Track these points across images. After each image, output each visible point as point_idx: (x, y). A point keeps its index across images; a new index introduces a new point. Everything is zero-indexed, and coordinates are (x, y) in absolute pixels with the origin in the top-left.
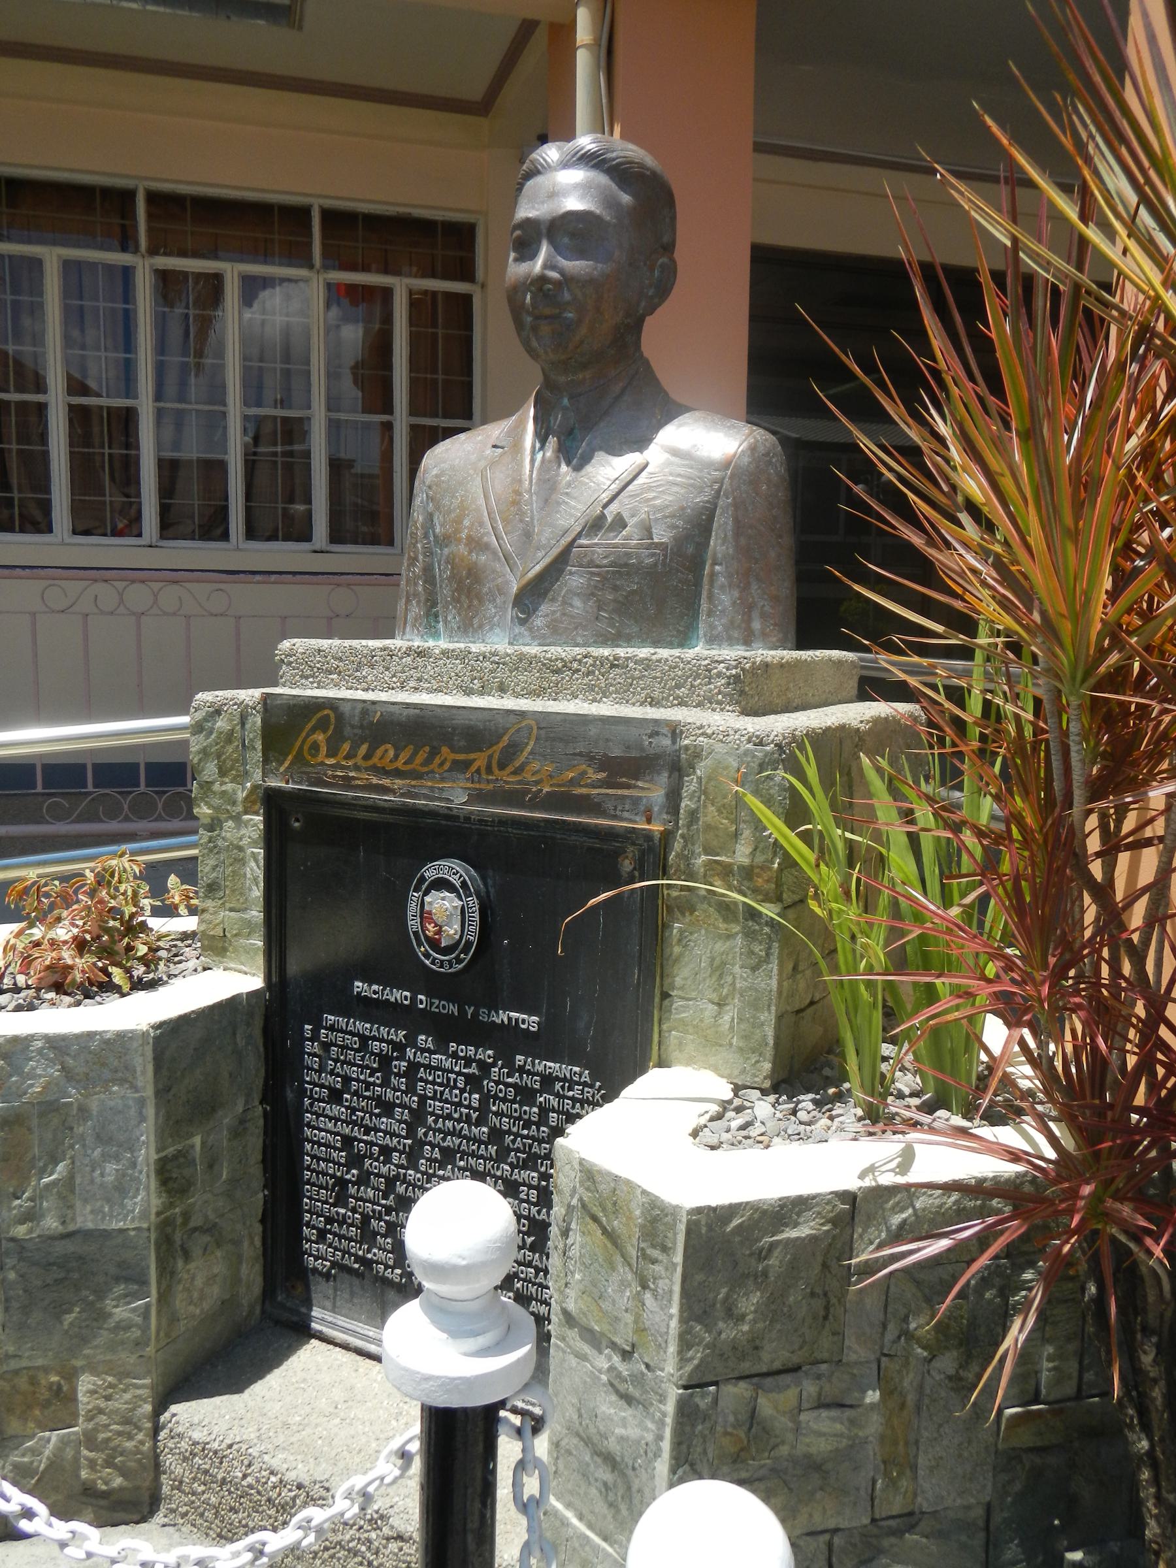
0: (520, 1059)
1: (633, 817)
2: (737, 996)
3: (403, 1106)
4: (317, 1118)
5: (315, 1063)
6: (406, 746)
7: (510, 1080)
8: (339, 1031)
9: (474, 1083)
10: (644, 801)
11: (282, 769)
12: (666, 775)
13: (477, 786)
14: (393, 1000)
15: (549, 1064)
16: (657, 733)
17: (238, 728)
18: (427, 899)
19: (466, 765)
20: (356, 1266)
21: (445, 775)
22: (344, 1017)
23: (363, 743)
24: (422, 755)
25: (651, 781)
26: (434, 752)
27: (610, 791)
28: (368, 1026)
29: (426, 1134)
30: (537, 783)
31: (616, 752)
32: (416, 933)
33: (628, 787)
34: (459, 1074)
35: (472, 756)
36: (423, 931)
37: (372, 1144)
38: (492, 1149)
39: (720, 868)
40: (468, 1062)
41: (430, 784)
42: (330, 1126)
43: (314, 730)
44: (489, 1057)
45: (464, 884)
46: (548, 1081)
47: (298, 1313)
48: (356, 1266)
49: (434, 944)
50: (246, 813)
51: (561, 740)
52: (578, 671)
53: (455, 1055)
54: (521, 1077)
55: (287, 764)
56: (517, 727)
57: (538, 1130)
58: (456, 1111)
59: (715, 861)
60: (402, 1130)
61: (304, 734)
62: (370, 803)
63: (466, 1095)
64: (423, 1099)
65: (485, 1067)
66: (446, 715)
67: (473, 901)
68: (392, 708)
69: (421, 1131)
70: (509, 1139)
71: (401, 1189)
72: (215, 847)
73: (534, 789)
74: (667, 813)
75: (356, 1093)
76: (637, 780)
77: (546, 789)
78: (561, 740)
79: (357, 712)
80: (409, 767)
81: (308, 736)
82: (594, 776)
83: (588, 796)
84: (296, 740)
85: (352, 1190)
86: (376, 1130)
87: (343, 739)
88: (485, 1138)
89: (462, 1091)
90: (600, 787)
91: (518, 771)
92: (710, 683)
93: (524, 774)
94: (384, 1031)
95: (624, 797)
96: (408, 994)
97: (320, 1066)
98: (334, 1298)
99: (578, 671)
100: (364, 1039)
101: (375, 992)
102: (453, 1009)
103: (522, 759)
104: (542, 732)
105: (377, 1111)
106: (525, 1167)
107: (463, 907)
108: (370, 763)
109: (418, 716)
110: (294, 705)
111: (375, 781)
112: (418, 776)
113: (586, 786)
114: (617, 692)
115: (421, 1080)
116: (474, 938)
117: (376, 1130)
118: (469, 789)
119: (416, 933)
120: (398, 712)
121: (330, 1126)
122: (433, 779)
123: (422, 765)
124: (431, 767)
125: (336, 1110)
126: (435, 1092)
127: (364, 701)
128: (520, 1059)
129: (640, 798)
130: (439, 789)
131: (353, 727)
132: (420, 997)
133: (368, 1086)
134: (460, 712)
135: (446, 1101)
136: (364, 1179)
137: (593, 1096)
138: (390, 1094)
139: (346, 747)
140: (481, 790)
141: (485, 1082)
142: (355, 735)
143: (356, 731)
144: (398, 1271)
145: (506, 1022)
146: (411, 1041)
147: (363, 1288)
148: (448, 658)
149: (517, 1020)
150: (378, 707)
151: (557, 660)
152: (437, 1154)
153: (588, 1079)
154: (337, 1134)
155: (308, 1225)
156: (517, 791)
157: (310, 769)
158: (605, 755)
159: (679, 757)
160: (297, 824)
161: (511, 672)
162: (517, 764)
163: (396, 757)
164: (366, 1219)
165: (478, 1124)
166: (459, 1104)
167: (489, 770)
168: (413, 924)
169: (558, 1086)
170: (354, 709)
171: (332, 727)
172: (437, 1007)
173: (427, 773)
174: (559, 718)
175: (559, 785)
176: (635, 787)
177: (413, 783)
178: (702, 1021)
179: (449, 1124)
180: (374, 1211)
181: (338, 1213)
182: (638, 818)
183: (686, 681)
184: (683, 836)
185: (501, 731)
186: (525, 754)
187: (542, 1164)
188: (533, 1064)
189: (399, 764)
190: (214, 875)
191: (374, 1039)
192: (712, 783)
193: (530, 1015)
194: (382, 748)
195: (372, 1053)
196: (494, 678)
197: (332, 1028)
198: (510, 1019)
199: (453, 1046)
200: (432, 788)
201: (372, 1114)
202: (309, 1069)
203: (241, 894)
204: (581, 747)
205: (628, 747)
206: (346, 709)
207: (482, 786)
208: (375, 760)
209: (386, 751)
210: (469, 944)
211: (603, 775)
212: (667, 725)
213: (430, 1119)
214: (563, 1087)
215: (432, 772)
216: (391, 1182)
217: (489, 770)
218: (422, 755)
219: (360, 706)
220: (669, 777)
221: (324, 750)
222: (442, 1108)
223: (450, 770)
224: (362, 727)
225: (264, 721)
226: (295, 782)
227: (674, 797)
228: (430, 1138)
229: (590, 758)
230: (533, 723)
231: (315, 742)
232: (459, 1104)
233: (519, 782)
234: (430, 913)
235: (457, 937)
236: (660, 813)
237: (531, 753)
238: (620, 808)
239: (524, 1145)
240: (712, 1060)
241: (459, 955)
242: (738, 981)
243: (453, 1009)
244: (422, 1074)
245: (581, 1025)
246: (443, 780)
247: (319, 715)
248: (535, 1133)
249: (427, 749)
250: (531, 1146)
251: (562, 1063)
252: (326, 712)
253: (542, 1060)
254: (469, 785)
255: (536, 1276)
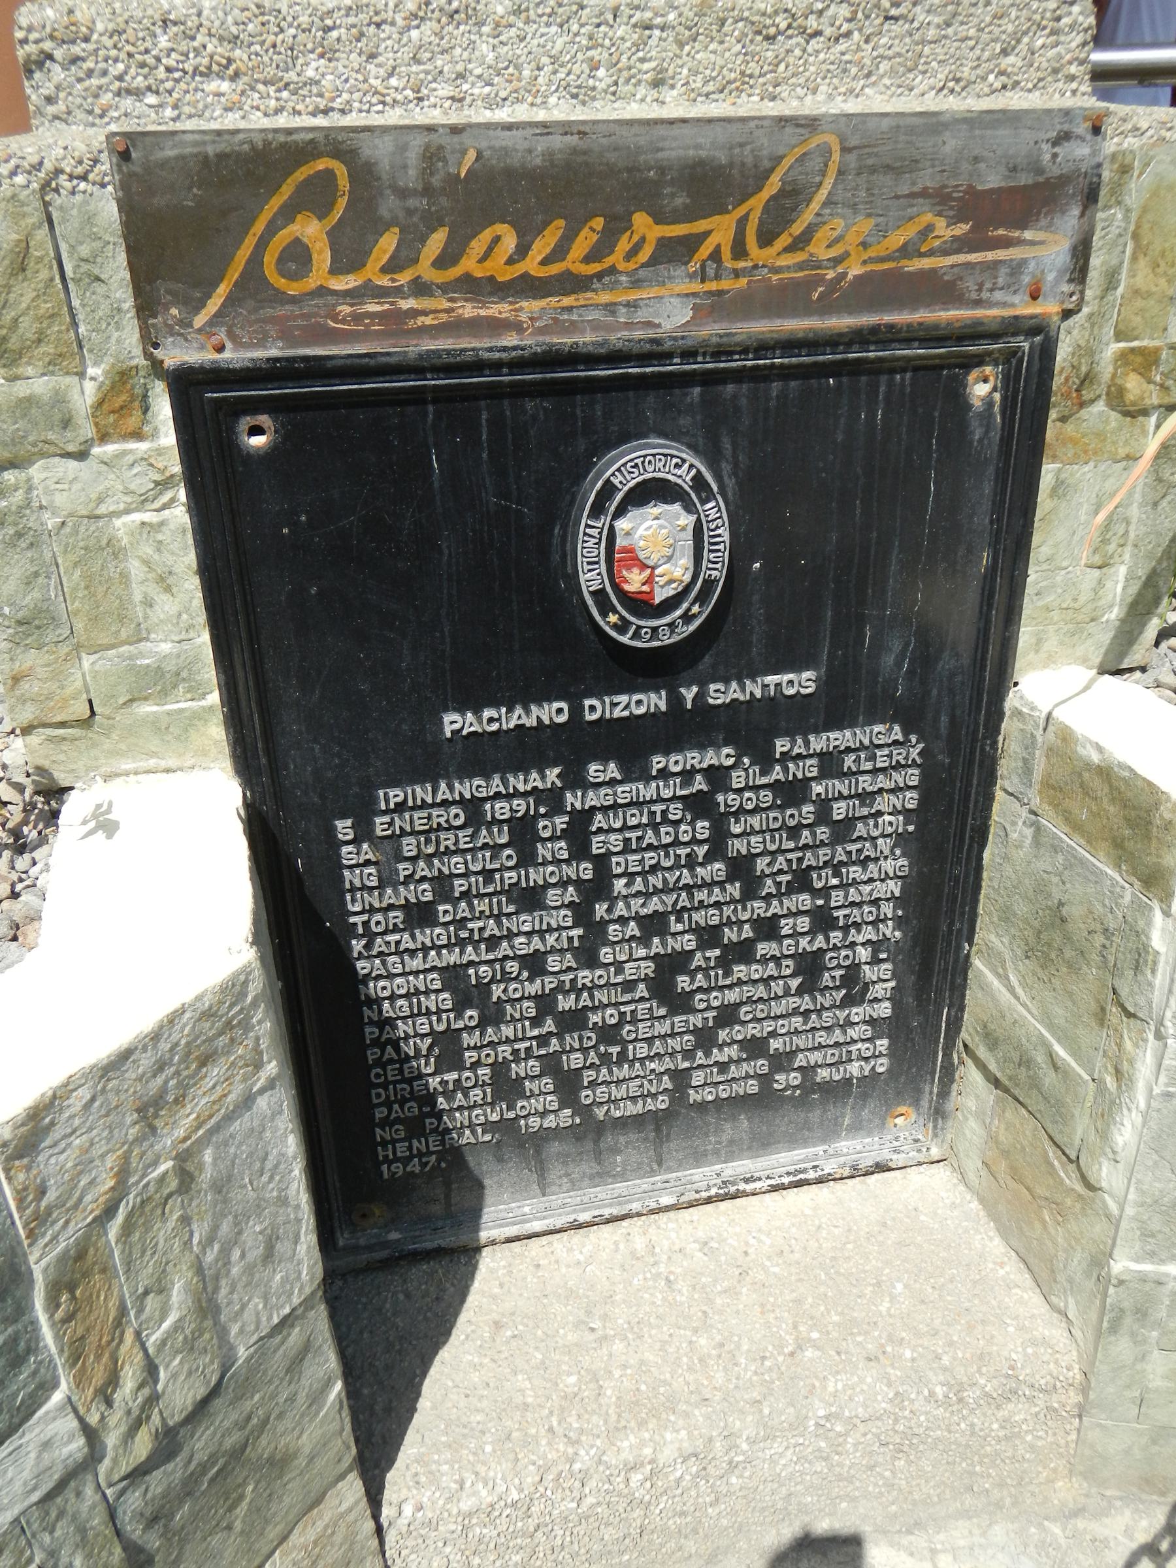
0: (781, 745)
1: (1009, 299)
2: (1128, 550)
3: (563, 884)
4: (384, 963)
5: (371, 876)
6: (546, 224)
7: (764, 780)
8: (414, 808)
9: (699, 805)
10: (1032, 266)
11: (200, 320)
12: (1076, 211)
13: (713, 286)
14: (531, 722)
15: (832, 735)
16: (1064, 137)
17: (43, 233)
18: (622, 524)
19: (691, 244)
20: (488, 1137)
21: (642, 273)
22: (422, 782)
23: (434, 230)
24: (585, 241)
25: (1048, 228)
26: (617, 225)
27: (974, 257)
28: (477, 782)
29: (609, 910)
30: (837, 261)
31: (992, 180)
32: (599, 595)
33: (1007, 243)
34: (675, 798)
35: (701, 225)
36: (616, 587)
37: (506, 958)
38: (734, 889)
39: (1139, 359)
40: (687, 775)
41: (605, 297)
42: (416, 963)
43: (288, 213)
44: (728, 756)
45: (699, 482)
46: (830, 764)
47: (385, 1244)
48: (488, 1137)
49: (640, 605)
50: (104, 437)
51: (888, 168)
52: (818, 33)
53: (664, 774)
54: (786, 770)
55: (214, 304)
56: (799, 151)
57: (814, 834)
58: (667, 855)
59: (1132, 350)
60: (564, 917)
61: (259, 227)
62: (469, 356)
63: (683, 827)
64: (602, 862)
65: (717, 776)
66: (642, 141)
67: (714, 511)
68: (506, 139)
69: (600, 909)
70: (761, 864)
71: (565, 1003)
72: (19, 535)
73: (831, 275)
74: (1071, 281)
75: (465, 895)
76: (1024, 227)
77: (855, 270)
78: (888, 168)
79: (413, 156)
80: (555, 269)
81: (272, 229)
82: (945, 231)
83: (933, 271)
84: (238, 244)
85: (467, 1039)
86: (510, 936)
87: (379, 227)
88: (722, 875)
89: (676, 823)
90: (958, 251)
91: (801, 242)
92: (1057, 44)
93: (811, 248)
94: (518, 782)
95: (997, 263)
96: (564, 705)
97: (380, 879)
98: (448, 1197)
99: (818, 33)
100: (473, 808)
101: (491, 720)
102: (656, 701)
103: (808, 216)
104: (852, 158)
105: (511, 909)
106: (791, 889)
107: (699, 520)
108: (455, 272)
109: (575, 151)
110: (222, 156)
111: (468, 310)
112: (573, 284)
113: (931, 253)
114: (892, 72)
115: (600, 830)
116: (719, 573)
117: (510, 936)
118: (694, 295)
119: (599, 595)
120: (522, 145)
121: (416, 963)
122: (612, 287)
123: (587, 259)
124: (608, 261)
125: (424, 937)
126: (627, 841)
127: (431, 129)
128: (781, 745)
129: (1024, 262)
130: (628, 305)
131: (403, 193)
132: (587, 703)
133: (488, 875)
134: (676, 131)
135: (650, 847)
136: (492, 1016)
137: (906, 758)
138: (535, 876)
139: (388, 243)
140: (720, 293)
141: (720, 798)
142: (410, 212)
143: (412, 202)
144: (568, 1112)
145: (758, 695)
146: (575, 779)
147: (500, 1160)
148: (527, 21)
149: (778, 685)
150: (466, 139)
151: (776, 13)
152: (633, 929)
153: (900, 737)
154: (433, 969)
155: (386, 1123)
156: (796, 284)
157: (282, 311)
158: (971, 190)
159: (1100, 176)
160: (258, 441)
161: (681, 45)
162: (797, 229)
163: (522, 250)
164: (499, 1069)
165: (709, 858)
166: (676, 843)
167: (739, 250)
168: (590, 578)
169: (849, 761)
170: (403, 148)
171: (342, 203)
172: (627, 706)
173: (600, 276)
174: (885, 123)
175: (882, 260)
176: (1020, 242)
177: (567, 301)
178: (1075, 600)
179: (655, 881)
180: (515, 1052)
181: (444, 1083)
182: (1016, 299)
183: (1018, 41)
184: (1090, 316)
185: (766, 164)
186: (815, 206)
187: (820, 878)
188: (807, 743)
189: (531, 265)
190: (36, 594)
191: (498, 796)
192: (1149, 217)
193: (798, 668)
194: (487, 235)
195: (495, 821)
196: (642, 60)
197: (401, 807)
198: (765, 686)
199: (658, 762)
200: (610, 308)
201: (498, 918)
202: (353, 890)
203: (121, 619)
204: (927, 179)
205: (1014, 169)
206: (380, 151)
207: (725, 284)
208: (469, 264)
209: (497, 240)
210: (709, 584)
211: (962, 228)
212: (1086, 119)
213: (619, 884)
214: (857, 760)
215: (612, 270)
216: (545, 1003)
217: (739, 250)
218: (585, 241)
219: (417, 142)
220: (1082, 215)
221: (322, 258)
222: (642, 861)
223: (653, 262)
224: (428, 191)
225: (126, 206)
226: (238, 344)
227: (1082, 252)
228: (620, 909)
229: (940, 198)
230: (833, 141)
231: (297, 241)
232: (676, 843)
233: (800, 267)
234: (630, 550)
235: (687, 578)
236: (1057, 281)
237: (825, 204)
238: (988, 285)
239: (789, 861)
240: (1080, 651)
241: (689, 609)
242: (1132, 528)
243: (656, 701)
244: (599, 821)
245: (889, 660)
246: (636, 284)
247: (302, 174)
248: (810, 841)
249: (598, 223)
250: (800, 860)
251: (852, 725)
252: (321, 165)
253: (817, 731)
254: (696, 287)
255: (805, 1023)
